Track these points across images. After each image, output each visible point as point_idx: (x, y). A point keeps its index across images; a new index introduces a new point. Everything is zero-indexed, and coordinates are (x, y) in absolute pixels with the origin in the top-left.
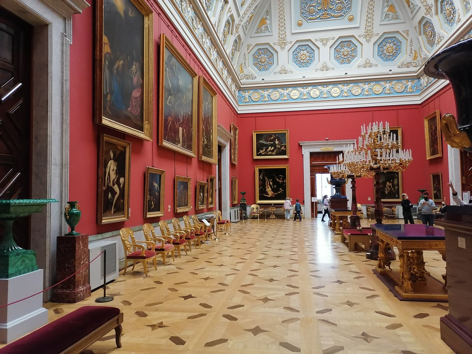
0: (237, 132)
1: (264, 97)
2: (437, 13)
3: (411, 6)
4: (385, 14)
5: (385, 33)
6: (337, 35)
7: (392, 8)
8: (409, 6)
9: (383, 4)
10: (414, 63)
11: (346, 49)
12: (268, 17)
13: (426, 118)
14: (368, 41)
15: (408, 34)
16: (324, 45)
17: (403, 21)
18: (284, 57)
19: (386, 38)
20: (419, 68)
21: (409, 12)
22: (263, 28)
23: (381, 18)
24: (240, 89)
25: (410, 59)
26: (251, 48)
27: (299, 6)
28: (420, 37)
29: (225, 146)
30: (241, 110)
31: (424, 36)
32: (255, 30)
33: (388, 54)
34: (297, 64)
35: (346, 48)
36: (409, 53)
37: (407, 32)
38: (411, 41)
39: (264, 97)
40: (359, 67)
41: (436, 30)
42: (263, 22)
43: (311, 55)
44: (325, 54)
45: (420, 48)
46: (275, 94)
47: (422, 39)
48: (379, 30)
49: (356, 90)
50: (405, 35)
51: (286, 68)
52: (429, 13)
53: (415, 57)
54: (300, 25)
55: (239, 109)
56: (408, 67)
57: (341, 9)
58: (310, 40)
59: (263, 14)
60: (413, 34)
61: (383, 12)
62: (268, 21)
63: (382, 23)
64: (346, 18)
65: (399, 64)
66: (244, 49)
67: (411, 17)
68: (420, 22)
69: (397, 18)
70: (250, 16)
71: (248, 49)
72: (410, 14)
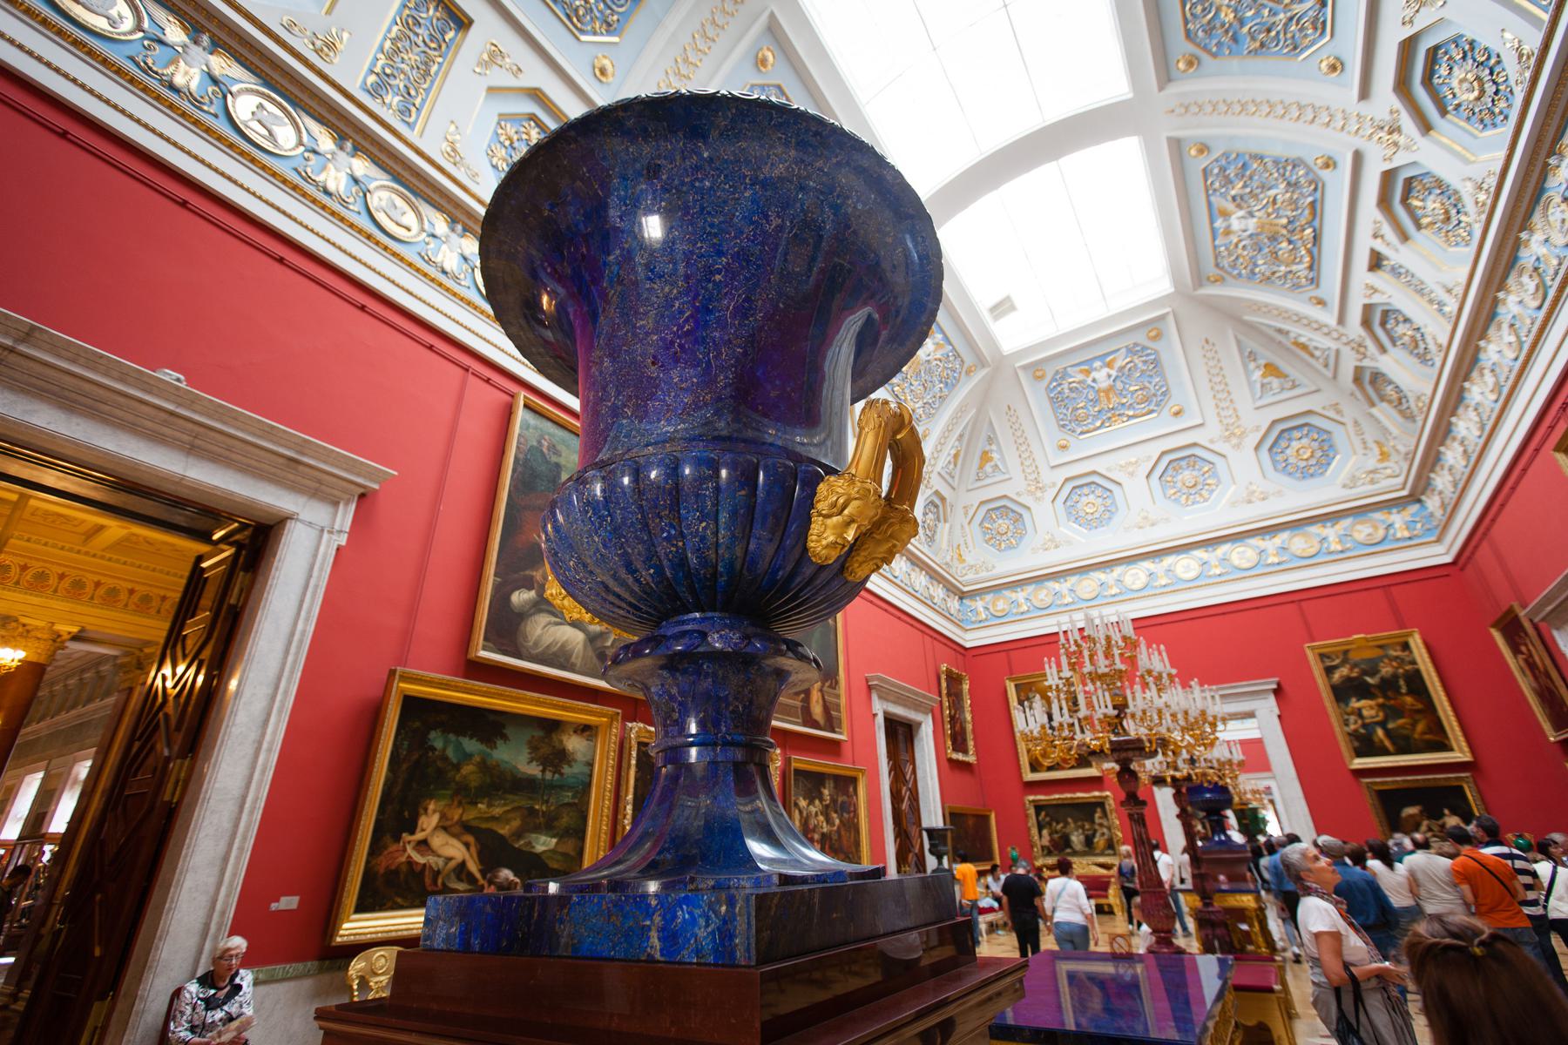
0: (966, 687)
1: (1019, 605)
2: (1383, 350)
3: (1317, 353)
4: (1258, 386)
5: (1274, 422)
6: (1155, 450)
7: (1271, 369)
8: (1312, 355)
9: (1245, 366)
11: (1187, 476)
12: (994, 447)
14: (1238, 446)
15: (1339, 412)
16: (1132, 474)
17: (1313, 388)
18: (1044, 515)
19: (1283, 431)
20: (1401, 479)
21: (1319, 365)
22: (988, 468)
23: (1253, 395)
24: (962, 596)
25: (1372, 462)
26: (971, 514)
27: (1049, 412)
28: (1374, 411)
29: (919, 724)
30: (971, 640)
31: (1384, 405)
32: (973, 476)
35: (1187, 473)
36: (1360, 451)
37: (1335, 407)
38: (1356, 423)
39: (1019, 605)
40: (1233, 504)
41: (1403, 387)
42: (985, 457)
43: (1109, 502)
44: (1137, 494)
45: (1385, 431)
46: (1043, 595)
47: (1384, 412)
48: (1256, 420)
49: (1242, 555)
50: (1332, 414)
51: (1054, 538)
52: (1365, 356)
53: (1384, 456)
54: (1064, 447)
55: (969, 636)
56: (1372, 482)
57: (1147, 400)
58: (1094, 472)
59: (981, 445)
60: (1351, 411)
61: (1251, 384)
62: (995, 455)
63: (1259, 403)
64: (1165, 412)
65: (1343, 476)
66: (958, 518)
67: (1329, 374)
68: (1357, 380)
69: (1294, 386)
70: (953, 452)
71: (966, 514)
72: (1324, 370)
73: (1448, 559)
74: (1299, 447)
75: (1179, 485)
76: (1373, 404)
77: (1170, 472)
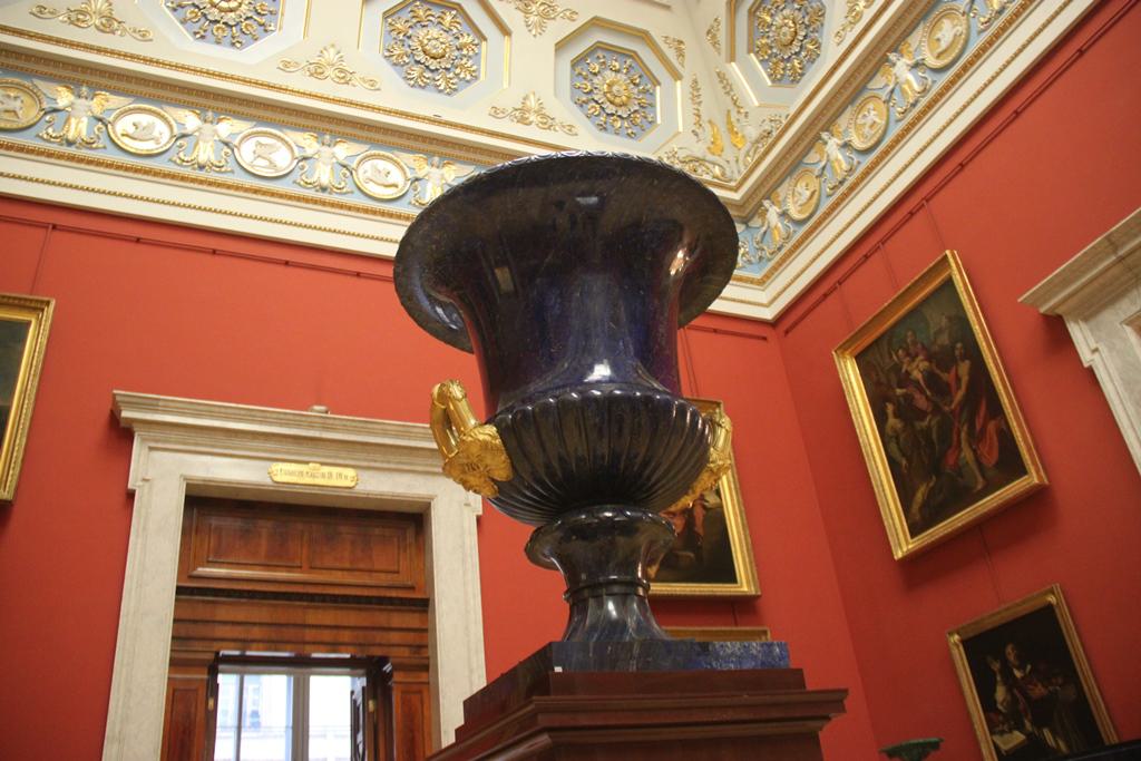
5: (596, 23)
10: (714, 164)
13: (843, 348)
15: (681, 54)
33: (611, 109)
34: (183, 22)
38: (695, 82)
50: (671, 54)
73: (768, 314)
74: (613, 80)
75: (415, 44)
76: (732, 58)
77: (406, 15)
